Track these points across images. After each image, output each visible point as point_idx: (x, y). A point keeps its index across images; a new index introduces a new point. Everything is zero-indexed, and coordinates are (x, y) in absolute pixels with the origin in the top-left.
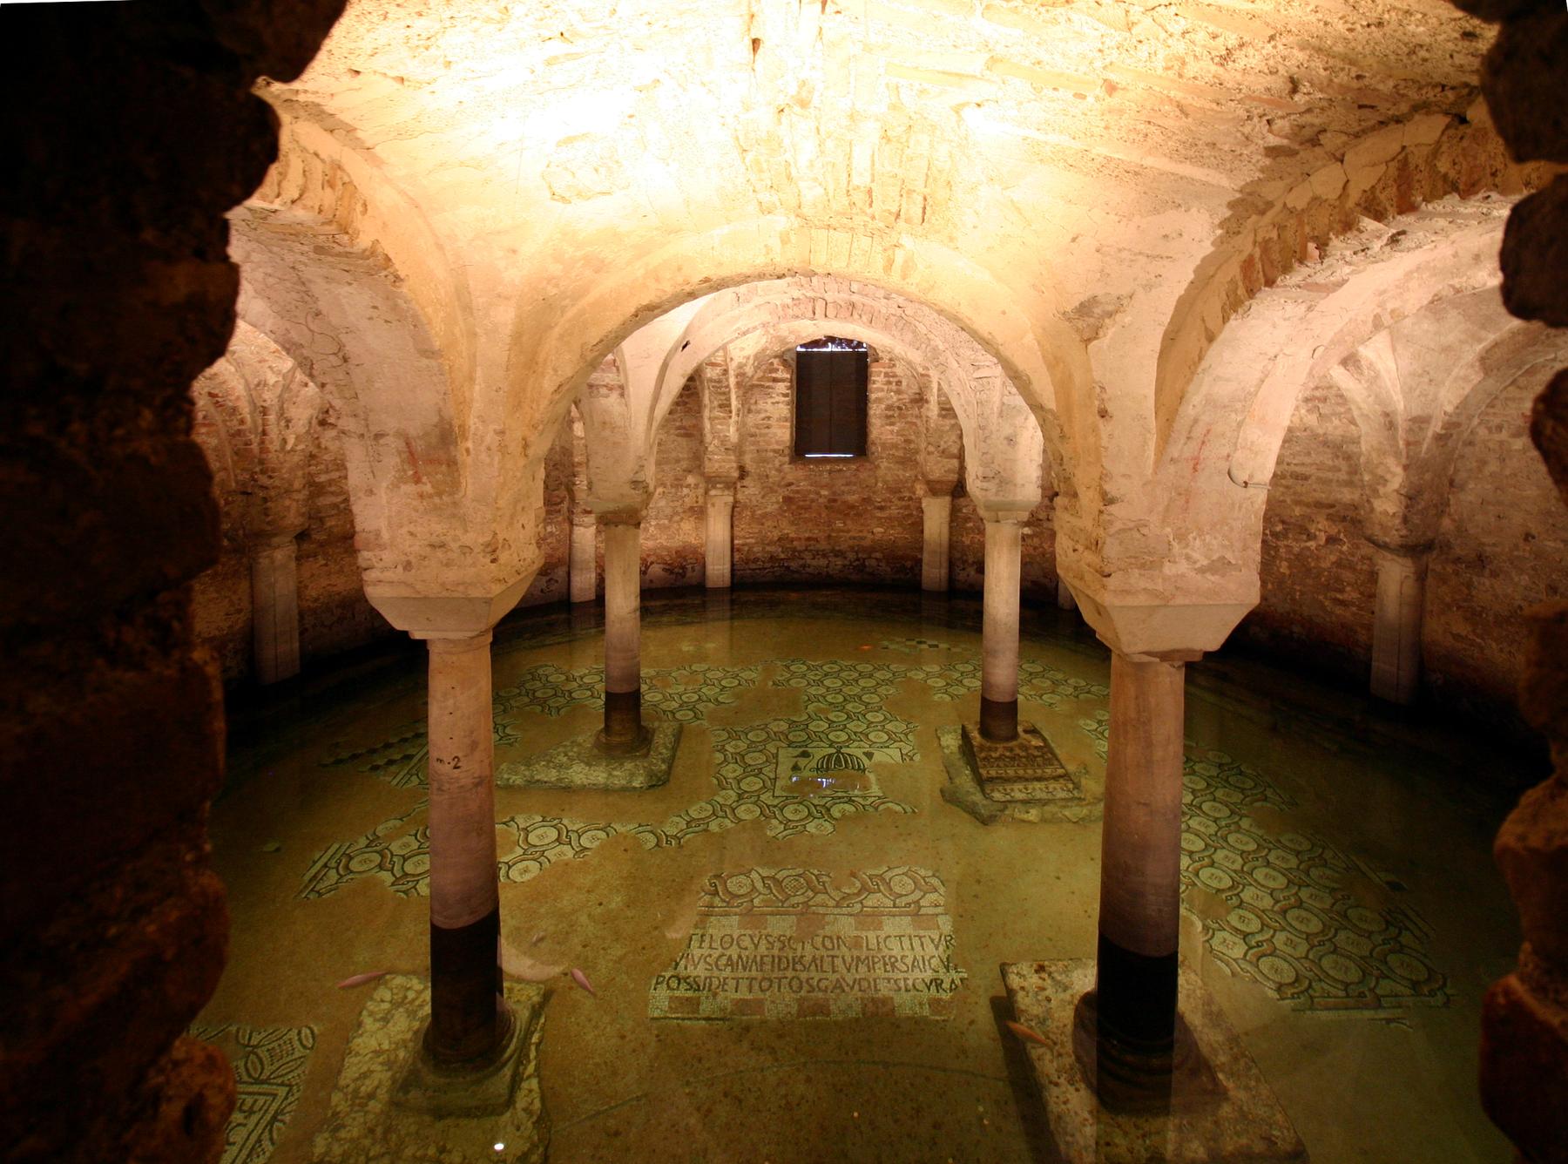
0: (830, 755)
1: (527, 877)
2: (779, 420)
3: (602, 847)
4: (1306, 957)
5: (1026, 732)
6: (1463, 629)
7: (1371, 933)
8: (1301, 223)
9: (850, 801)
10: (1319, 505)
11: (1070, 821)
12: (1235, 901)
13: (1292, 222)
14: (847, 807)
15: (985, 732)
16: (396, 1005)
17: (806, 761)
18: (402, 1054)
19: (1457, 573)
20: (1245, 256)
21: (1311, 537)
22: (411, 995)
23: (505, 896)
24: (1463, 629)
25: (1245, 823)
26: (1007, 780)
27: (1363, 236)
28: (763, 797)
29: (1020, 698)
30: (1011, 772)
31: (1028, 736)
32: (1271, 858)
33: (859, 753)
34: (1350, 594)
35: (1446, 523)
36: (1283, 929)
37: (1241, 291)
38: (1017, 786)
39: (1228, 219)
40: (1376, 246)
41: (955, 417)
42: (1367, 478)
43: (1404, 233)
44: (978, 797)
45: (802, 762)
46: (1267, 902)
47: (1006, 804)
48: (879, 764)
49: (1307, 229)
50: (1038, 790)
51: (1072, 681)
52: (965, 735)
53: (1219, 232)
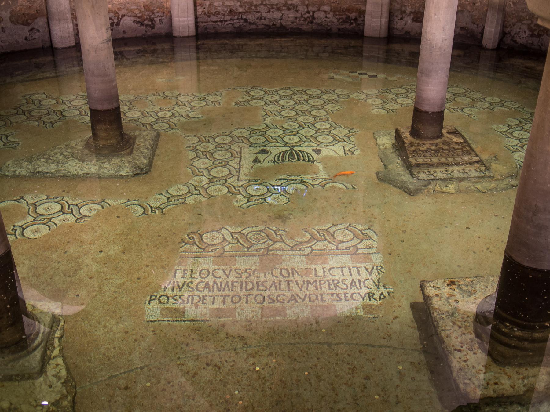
0: (285, 152)
1: (38, 235)
9: (302, 182)
11: (480, 191)
14: (299, 186)
15: (414, 132)
17: (265, 156)
26: (432, 165)
28: (229, 181)
30: (435, 160)
38: (438, 170)
44: (406, 177)
47: (429, 182)
50: (456, 171)
52: (398, 136)
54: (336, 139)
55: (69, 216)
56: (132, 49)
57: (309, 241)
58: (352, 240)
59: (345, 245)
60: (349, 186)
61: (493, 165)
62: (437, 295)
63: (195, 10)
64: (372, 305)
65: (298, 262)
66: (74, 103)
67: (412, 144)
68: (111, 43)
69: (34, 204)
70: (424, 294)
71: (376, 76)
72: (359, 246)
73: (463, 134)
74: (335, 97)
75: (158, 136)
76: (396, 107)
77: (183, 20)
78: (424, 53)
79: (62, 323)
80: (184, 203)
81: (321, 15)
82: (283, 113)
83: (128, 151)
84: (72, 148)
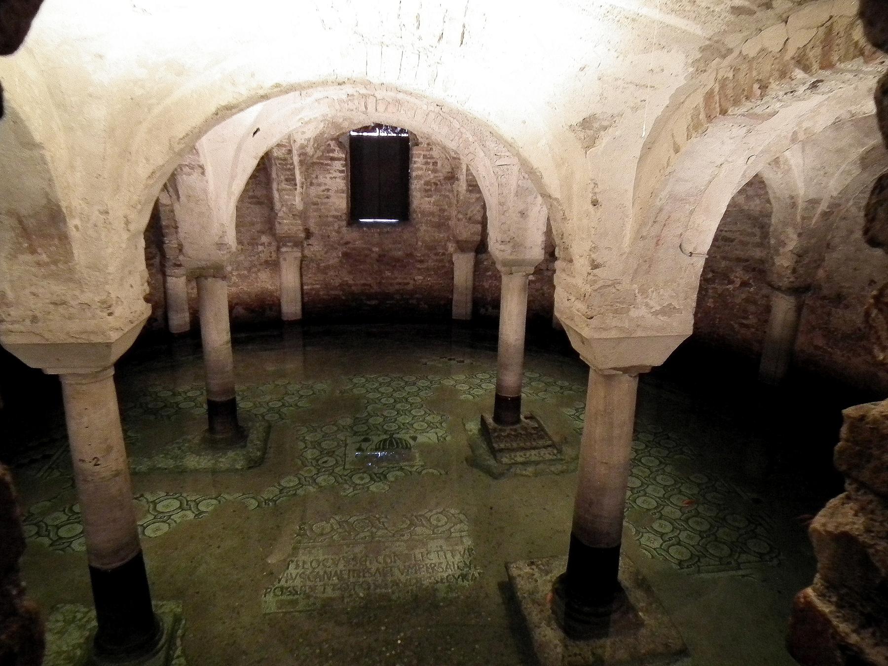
0: (385, 440)
2: (337, 191)
3: (215, 510)
4: (698, 544)
5: (526, 418)
6: (820, 342)
7: (739, 528)
8: (750, 69)
9: (401, 469)
10: (739, 260)
12: (658, 515)
13: (744, 67)
15: (497, 419)
16: (67, 622)
17: (367, 444)
18: (79, 652)
19: (823, 307)
20: (708, 88)
21: (731, 282)
22: (79, 616)
23: (144, 546)
24: (820, 342)
25: (668, 469)
27: (794, 82)
28: (336, 470)
29: (523, 395)
30: (515, 445)
31: (527, 421)
32: (683, 489)
33: (407, 437)
34: (752, 320)
35: (821, 273)
36: (686, 530)
37: (702, 116)
39: (698, 61)
40: (801, 89)
41: (479, 192)
42: (772, 241)
43: (822, 81)
44: (492, 462)
45: (364, 445)
46: (678, 514)
48: (422, 444)
49: (754, 73)
50: (533, 455)
51: (559, 383)
53: (691, 70)
54: (431, 425)
55: (189, 512)
56: (243, 335)
57: (408, 528)
58: (446, 523)
59: (441, 529)
60: (443, 472)
61: (564, 448)
62: (519, 575)
63: (302, 298)
64: (464, 587)
65: (400, 547)
66: (190, 394)
67: (495, 430)
68: (230, 345)
69: (154, 502)
70: (509, 575)
71: (463, 362)
72: (452, 530)
73: (538, 418)
74: (427, 383)
75: (270, 427)
76: (481, 392)
77: (291, 308)
78: (501, 349)
79: (184, 622)
80: (295, 494)
81: (414, 302)
82: (383, 401)
83: (242, 444)
84: (189, 441)
